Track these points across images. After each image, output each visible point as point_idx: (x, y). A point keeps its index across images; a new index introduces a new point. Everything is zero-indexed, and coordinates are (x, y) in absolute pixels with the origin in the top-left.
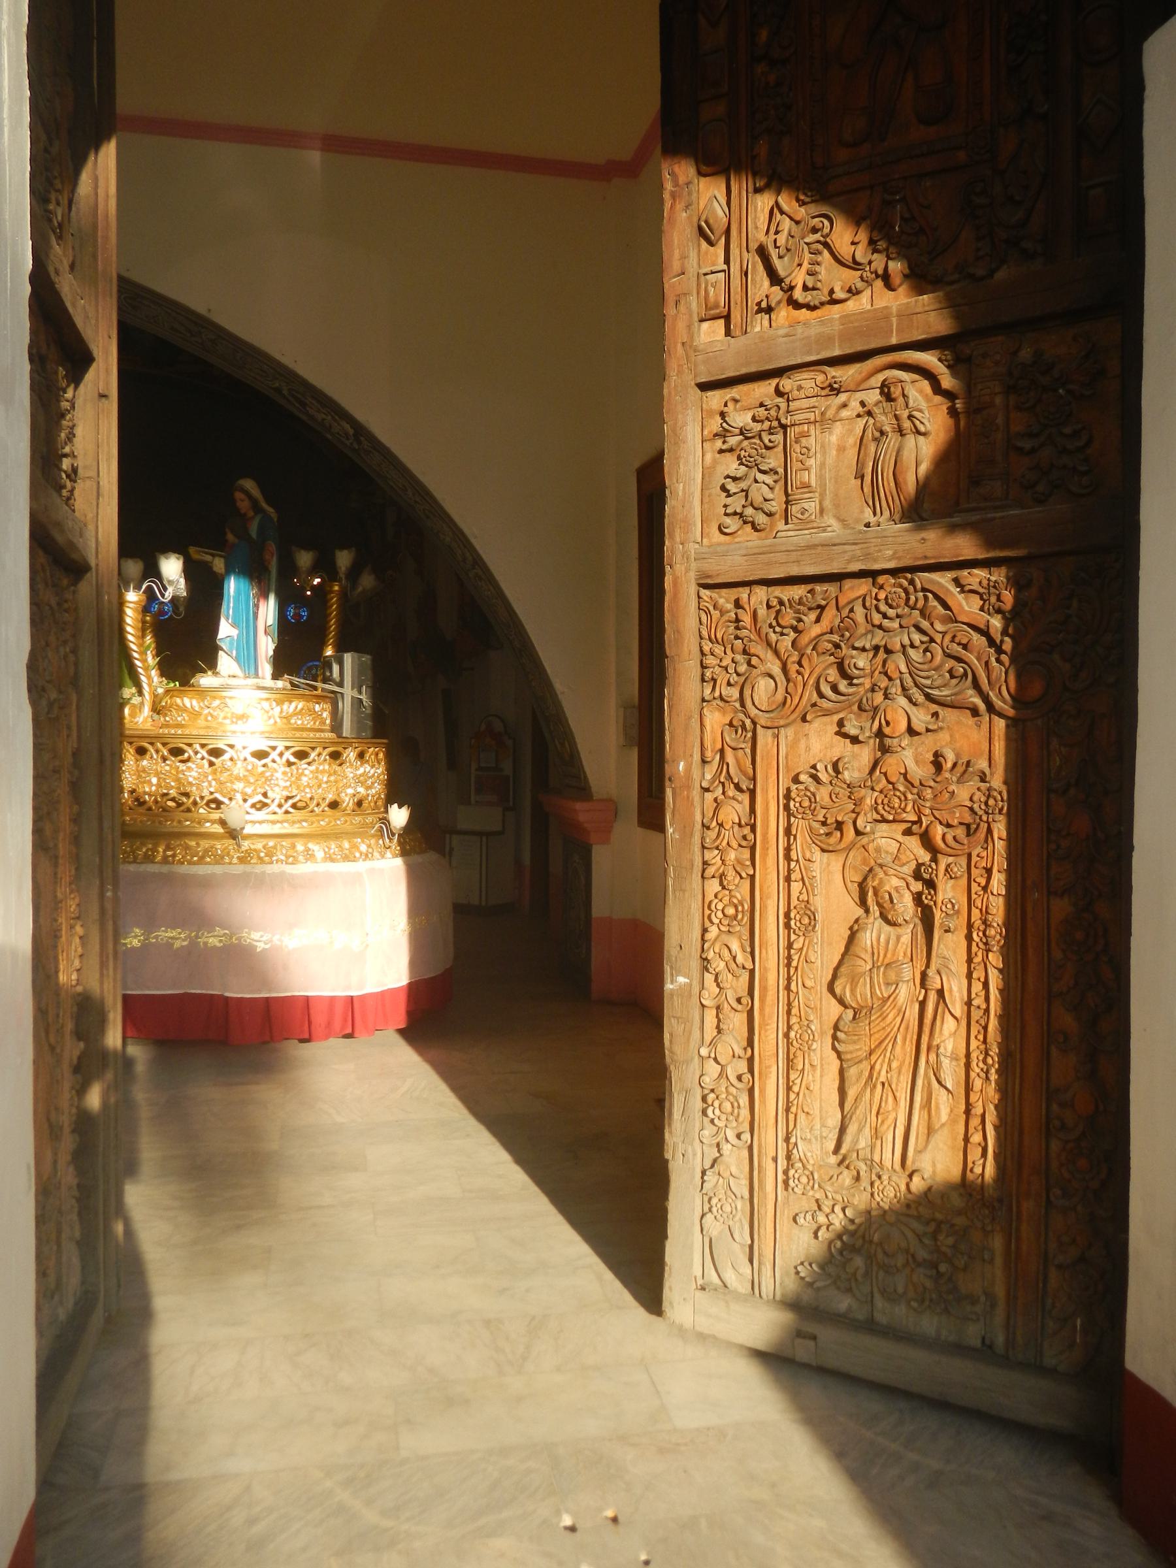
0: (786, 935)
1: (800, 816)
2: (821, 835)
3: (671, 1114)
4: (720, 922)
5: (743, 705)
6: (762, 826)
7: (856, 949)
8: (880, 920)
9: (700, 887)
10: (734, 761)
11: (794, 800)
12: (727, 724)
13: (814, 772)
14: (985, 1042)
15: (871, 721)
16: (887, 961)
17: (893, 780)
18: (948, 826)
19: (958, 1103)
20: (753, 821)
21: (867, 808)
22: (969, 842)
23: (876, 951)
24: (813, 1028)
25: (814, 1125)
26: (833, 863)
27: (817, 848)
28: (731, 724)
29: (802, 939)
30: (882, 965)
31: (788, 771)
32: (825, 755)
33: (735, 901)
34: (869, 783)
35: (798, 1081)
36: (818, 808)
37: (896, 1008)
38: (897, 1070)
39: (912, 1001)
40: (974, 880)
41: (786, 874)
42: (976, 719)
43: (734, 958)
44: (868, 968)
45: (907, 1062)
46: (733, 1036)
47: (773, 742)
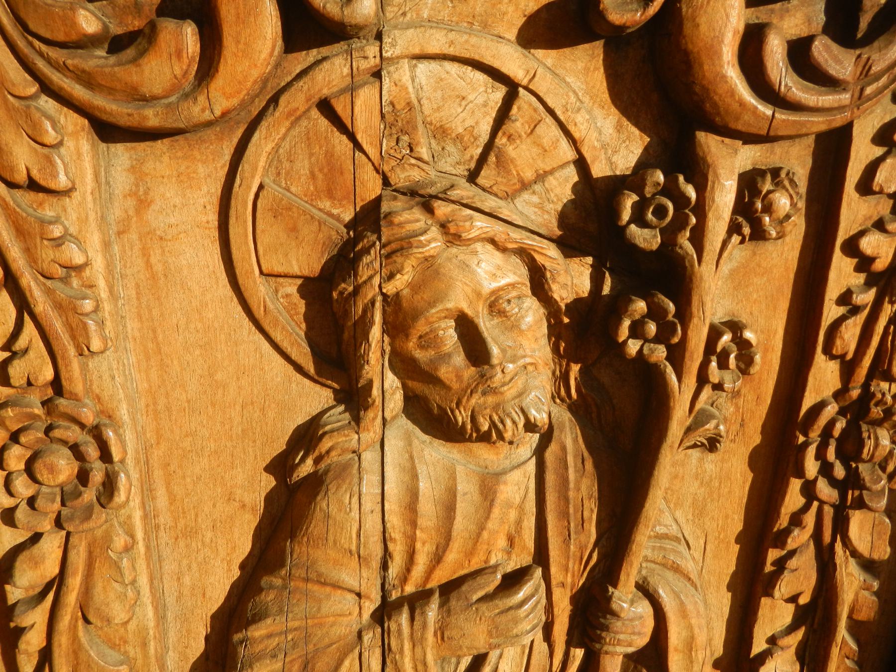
2: (85, 43)
8: (404, 423)
16: (441, 576)
22: (865, 74)
23: (398, 551)
27: (71, 120)
30: (423, 596)
40: (852, 247)
44: (370, 607)
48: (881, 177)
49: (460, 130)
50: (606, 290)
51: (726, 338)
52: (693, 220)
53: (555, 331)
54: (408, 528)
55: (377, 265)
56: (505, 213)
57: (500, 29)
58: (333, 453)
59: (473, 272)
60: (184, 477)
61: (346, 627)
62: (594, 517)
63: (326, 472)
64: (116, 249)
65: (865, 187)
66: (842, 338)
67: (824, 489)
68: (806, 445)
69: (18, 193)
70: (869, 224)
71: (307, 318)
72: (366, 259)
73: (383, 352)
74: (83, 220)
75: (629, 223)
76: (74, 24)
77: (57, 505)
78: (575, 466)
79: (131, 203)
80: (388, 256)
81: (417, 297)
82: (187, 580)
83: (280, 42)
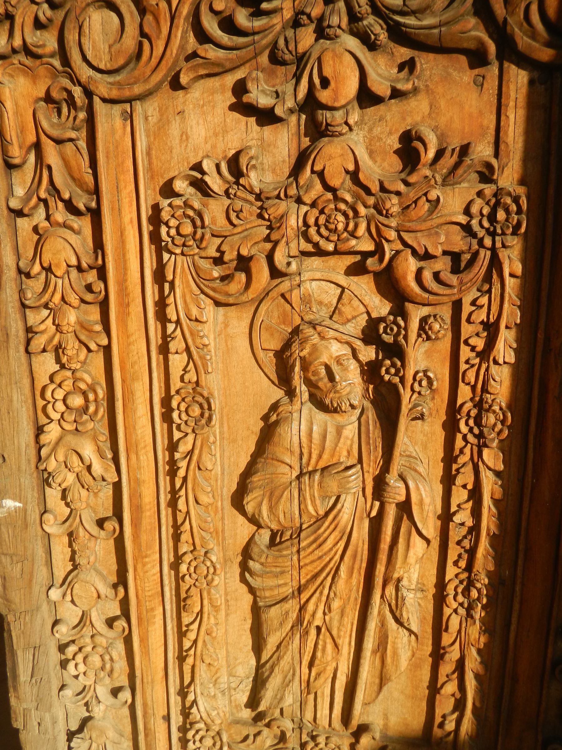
0: (166, 431)
1: (178, 251)
2: (214, 279)
3: (15, 676)
4: (62, 416)
5: (66, 61)
6: (117, 268)
7: (273, 449)
8: (309, 404)
9: (25, 367)
10: (60, 162)
11: (167, 224)
12: (41, 99)
13: (199, 176)
14: (469, 568)
15: (294, 81)
16: (321, 465)
17: (334, 182)
18: (427, 256)
19: (422, 644)
20: (100, 262)
21: (290, 233)
22: (461, 283)
23: (305, 451)
24: (214, 559)
25: (219, 678)
26: (234, 322)
27: (209, 301)
28: (48, 99)
29: (190, 438)
30: (315, 471)
31: (152, 177)
32: (214, 147)
33: (83, 386)
34: (293, 191)
35: (195, 626)
36: (208, 236)
37: (338, 529)
38: (339, 611)
39: (362, 519)
40: (466, 343)
41: (160, 341)
42: (476, 71)
43: (89, 468)
44: (295, 474)
45: (352, 599)
46: (96, 570)
47: (124, 127)
48: (473, 317)
50: (380, 357)
51: (421, 374)
52: (403, 332)
53: (362, 372)
56: (341, 330)
59: (329, 349)
61: (285, 479)
64: (217, 340)
65: (468, 321)
67: (470, 437)
69: (192, 322)
70: (474, 334)
72: (294, 345)
73: (300, 377)
74: (209, 331)
76: (212, 275)
77: (193, 424)
79: (223, 325)
80: (301, 344)
82: (232, 460)
83: (269, 278)
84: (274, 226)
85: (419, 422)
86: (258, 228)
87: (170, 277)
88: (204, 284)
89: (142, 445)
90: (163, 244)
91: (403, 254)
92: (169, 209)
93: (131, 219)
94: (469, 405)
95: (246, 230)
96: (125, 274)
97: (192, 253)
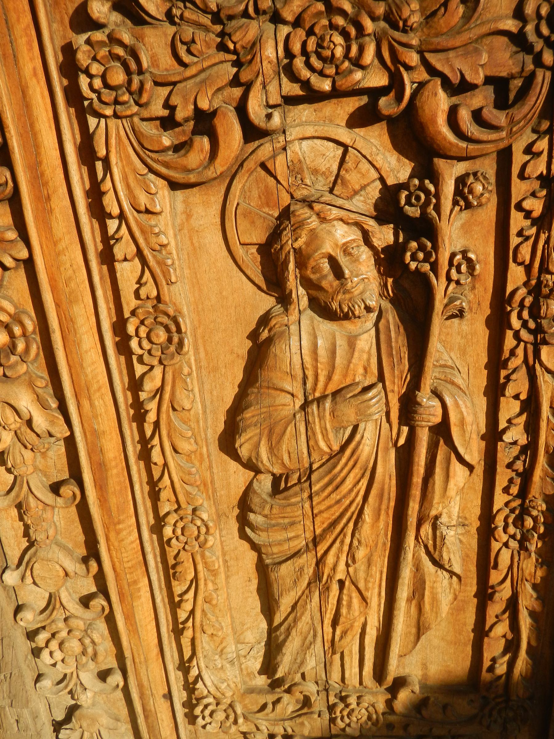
0: (124, 366)
2: (164, 150)
6: (24, 146)
8: (309, 312)
14: (523, 493)
16: (332, 388)
19: (466, 585)
22: (512, 122)
23: (310, 374)
24: (205, 516)
25: (225, 647)
26: (199, 210)
30: (324, 397)
36: (149, 85)
37: (358, 465)
38: (365, 560)
39: (387, 449)
40: (519, 207)
41: (100, 247)
43: (29, 423)
44: (299, 402)
45: (380, 545)
46: (58, 544)
48: (528, 170)
49: (324, 170)
50: (401, 240)
51: (459, 257)
52: (434, 201)
53: (378, 262)
54: (314, 362)
55: (290, 235)
56: (347, 206)
57: (338, 122)
58: (277, 326)
59: (334, 235)
60: (211, 342)
61: (287, 411)
62: (406, 356)
63: (274, 335)
64: (179, 237)
65: (522, 176)
66: (521, 253)
67: (524, 334)
68: (511, 311)
69: (141, 215)
70: (528, 194)
71: (261, 263)
73: (296, 277)
74: (166, 225)
75: (405, 205)
76: (161, 143)
77: (159, 353)
78: (395, 331)
79: (184, 216)
80: (294, 230)
81: (309, 249)
82: (215, 393)
83: (242, 140)
84: (243, 60)
85: (456, 321)
86: (220, 66)
87: (102, 152)
88: (152, 159)
89: (95, 386)
90: (86, 103)
91: (430, 86)
92: (86, 48)
93: (34, 69)
94: (523, 292)
95: (203, 70)
96: (38, 154)
97: (129, 113)
